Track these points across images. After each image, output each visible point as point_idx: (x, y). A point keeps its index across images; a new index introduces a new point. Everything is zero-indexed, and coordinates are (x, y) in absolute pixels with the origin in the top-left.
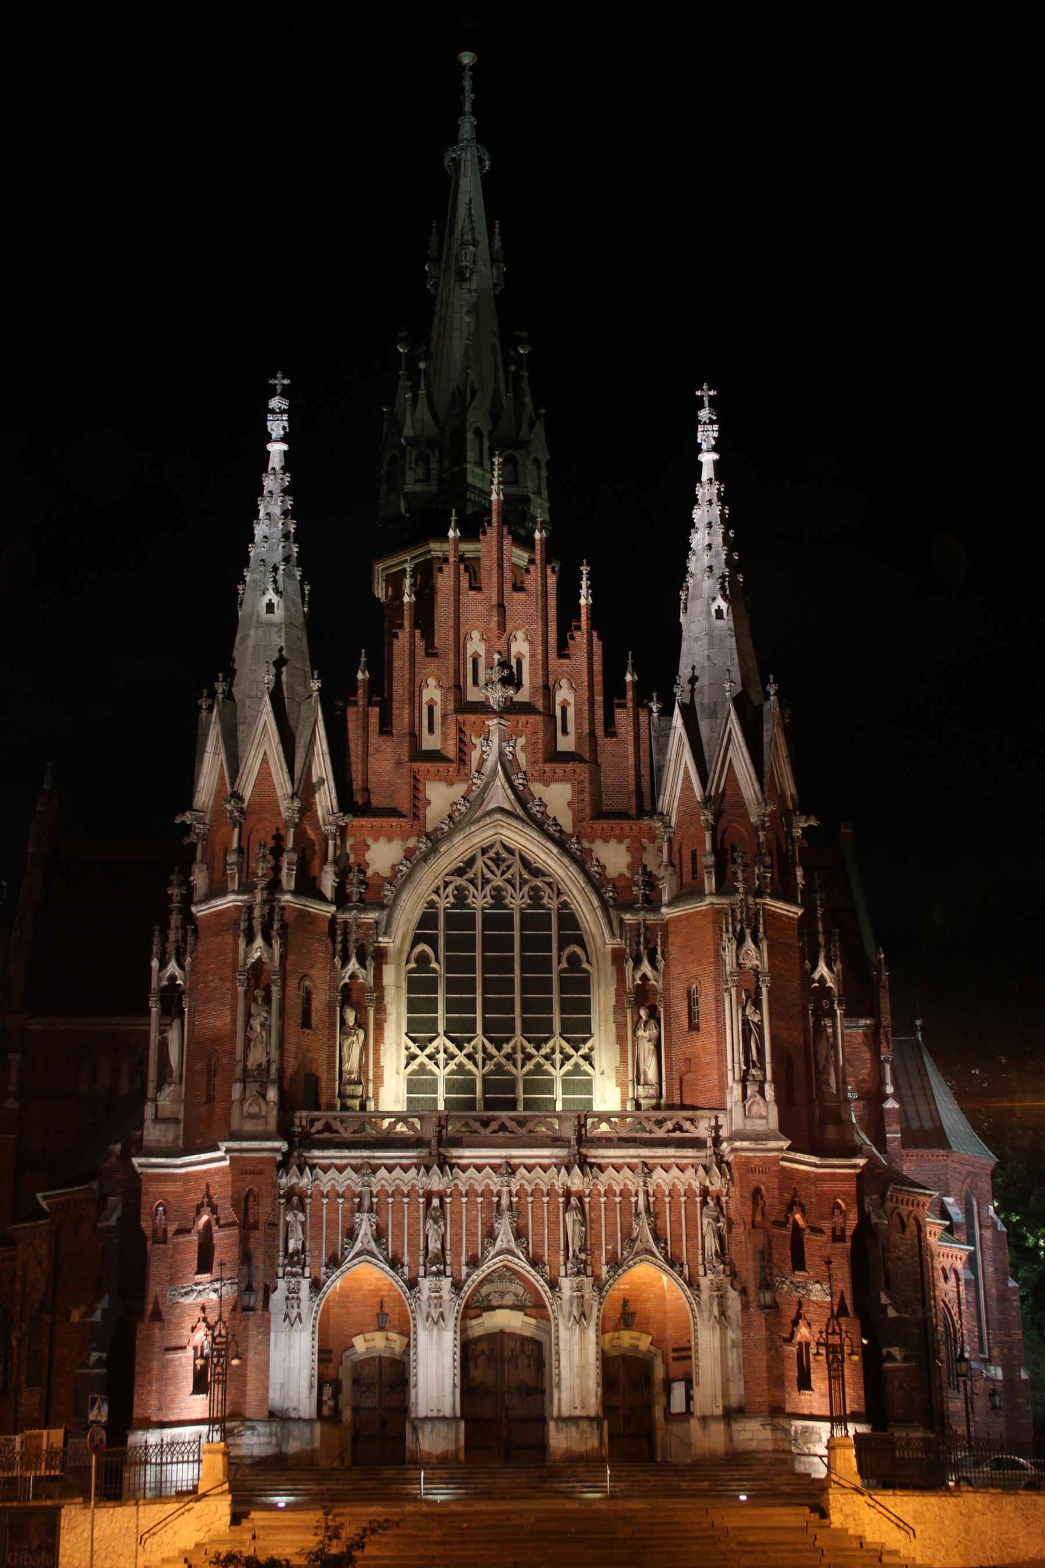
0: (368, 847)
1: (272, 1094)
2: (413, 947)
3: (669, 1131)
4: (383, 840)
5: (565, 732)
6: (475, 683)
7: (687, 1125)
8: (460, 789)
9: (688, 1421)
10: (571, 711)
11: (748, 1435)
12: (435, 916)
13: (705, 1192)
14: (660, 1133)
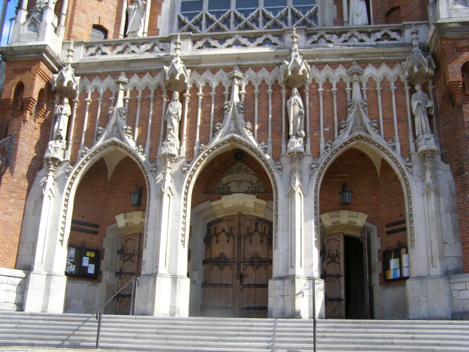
3: (378, 40)
7: (393, 35)
9: (404, 285)
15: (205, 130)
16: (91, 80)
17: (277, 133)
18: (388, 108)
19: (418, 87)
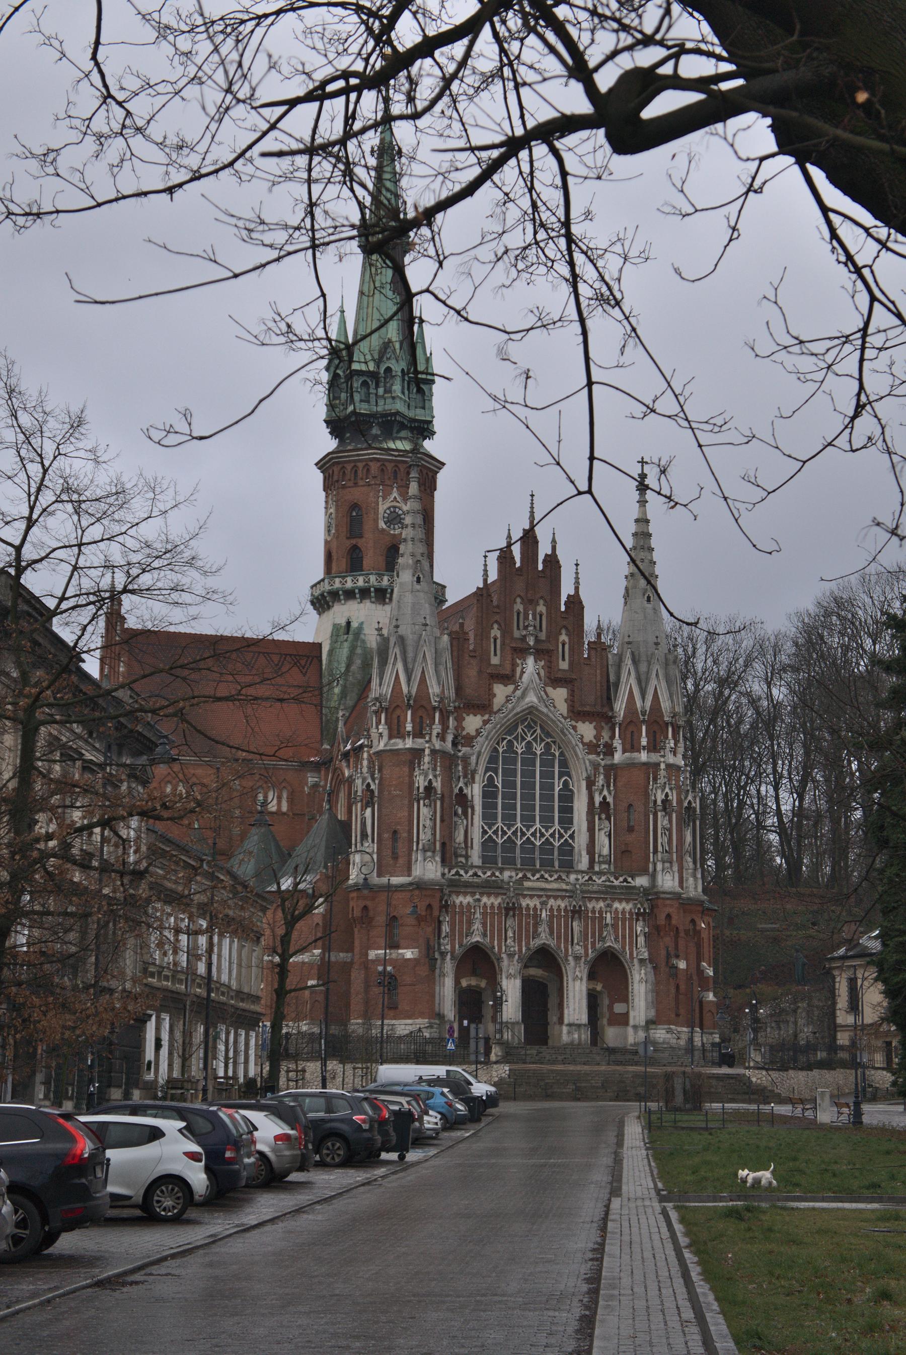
0: (464, 719)
1: (438, 859)
2: (485, 774)
4: (471, 716)
5: (563, 659)
6: (518, 628)
7: (630, 879)
8: (511, 688)
10: (567, 647)
11: (658, 1035)
12: (497, 757)
13: (637, 914)
14: (616, 883)
15: (527, 937)
16: (458, 896)
17: (566, 940)
18: (624, 929)
19: (641, 918)
